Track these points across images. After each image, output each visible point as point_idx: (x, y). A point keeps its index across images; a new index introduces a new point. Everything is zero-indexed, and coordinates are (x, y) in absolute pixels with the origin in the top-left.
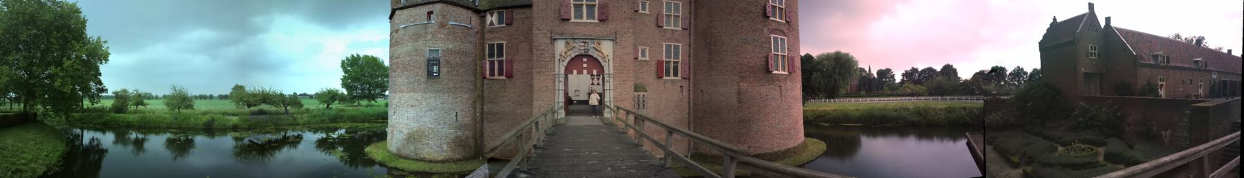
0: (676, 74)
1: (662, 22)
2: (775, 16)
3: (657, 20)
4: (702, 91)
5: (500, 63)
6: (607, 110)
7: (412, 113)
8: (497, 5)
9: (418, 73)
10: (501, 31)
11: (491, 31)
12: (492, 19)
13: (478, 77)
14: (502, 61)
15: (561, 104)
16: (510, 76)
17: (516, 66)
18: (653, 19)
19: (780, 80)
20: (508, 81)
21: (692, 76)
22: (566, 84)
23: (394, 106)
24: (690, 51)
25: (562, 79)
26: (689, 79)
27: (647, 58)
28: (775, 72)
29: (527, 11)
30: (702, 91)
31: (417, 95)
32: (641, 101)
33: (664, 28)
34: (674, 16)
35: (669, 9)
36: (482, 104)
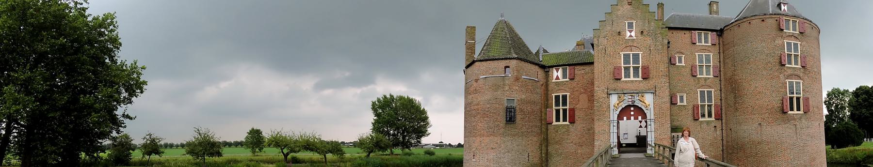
0: (710, 115)
1: (696, 72)
2: (790, 63)
4: (731, 129)
5: (565, 111)
7: (492, 155)
13: (543, 122)
14: (566, 109)
15: (615, 143)
16: (572, 121)
17: (577, 114)
18: (688, 70)
20: (571, 126)
22: (618, 128)
24: (721, 95)
25: (616, 124)
26: (722, 120)
30: (731, 129)
31: (496, 138)
33: (698, 76)
34: (706, 66)
35: (701, 61)
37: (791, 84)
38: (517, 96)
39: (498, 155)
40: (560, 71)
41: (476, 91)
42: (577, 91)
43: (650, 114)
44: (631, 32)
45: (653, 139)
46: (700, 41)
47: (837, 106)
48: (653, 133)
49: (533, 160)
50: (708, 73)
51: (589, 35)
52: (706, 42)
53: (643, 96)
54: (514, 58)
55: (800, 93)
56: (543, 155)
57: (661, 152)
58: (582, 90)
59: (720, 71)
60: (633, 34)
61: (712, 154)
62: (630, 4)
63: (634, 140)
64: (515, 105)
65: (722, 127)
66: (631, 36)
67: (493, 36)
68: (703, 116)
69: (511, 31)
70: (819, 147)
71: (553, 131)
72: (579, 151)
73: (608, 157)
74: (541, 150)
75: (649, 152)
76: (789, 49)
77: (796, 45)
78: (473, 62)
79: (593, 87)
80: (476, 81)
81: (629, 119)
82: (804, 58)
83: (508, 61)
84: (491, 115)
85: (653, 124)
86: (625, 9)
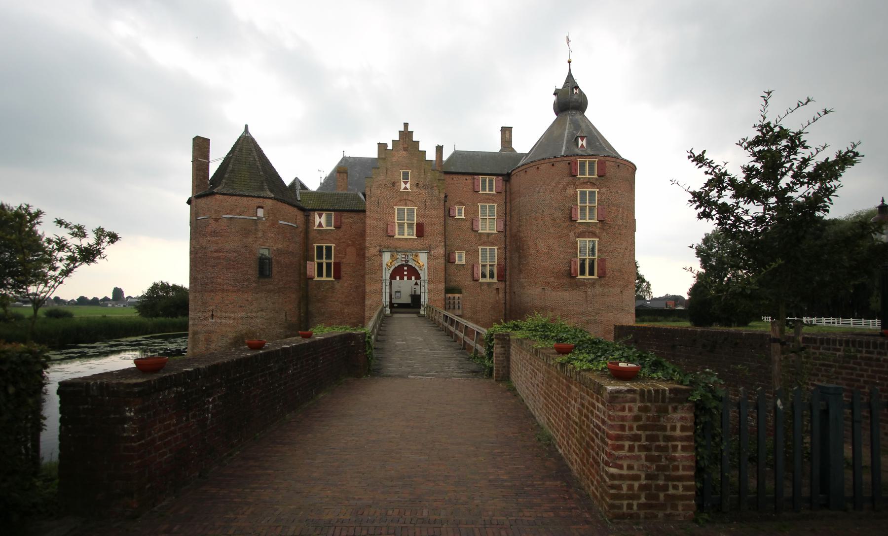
0: (492, 276)
3: (473, 224)
4: (514, 293)
5: (329, 265)
9: (247, 271)
10: (329, 233)
11: (320, 232)
14: (331, 263)
15: (387, 303)
16: (338, 276)
17: (344, 270)
20: (336, 283)
21: (508, 278)
25: (388, 284)
28: (580, 277)
31: (246, 296)
32: (456, 302)
39: (249, 314)
42: (344, 242)
43: (424, 275)
45: (426, 300)
48: (426, 294)
49: (291, 321)
56: (302, 315)
58: (350, 242)
61: (493, 318)
63: (406, 299)
65: (505, 290)
71: (315, 287)
72: (346, 311)
74: (300, 309)
75: (422, 312)
79: (364, 240)
81: (402, 278)
84: (239, 266)
85: (426, 284)
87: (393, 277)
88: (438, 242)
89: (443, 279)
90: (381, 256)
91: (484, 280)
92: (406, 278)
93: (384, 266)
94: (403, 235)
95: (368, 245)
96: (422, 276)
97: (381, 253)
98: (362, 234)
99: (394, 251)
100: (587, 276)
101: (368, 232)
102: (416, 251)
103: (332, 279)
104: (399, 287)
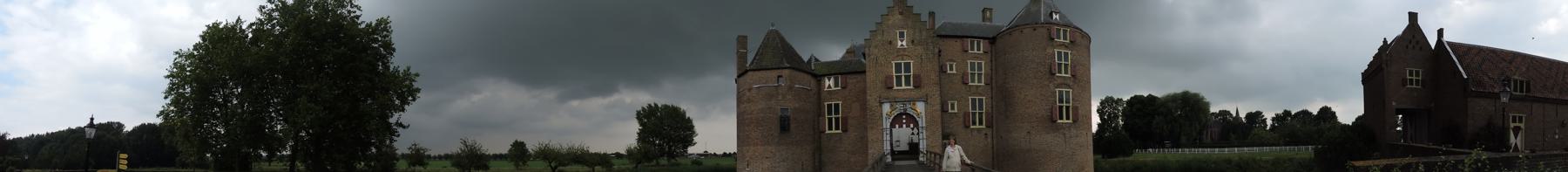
2: (1060, 72)
5: (837, 119)
6: (921, 155)
8: (833, 72)
12: (829, 83)
14: (838, 118)
16: (845, 130)
17: (850, 121)
19: (1064, 129)
22: (891, 136)
23: (748, 159)
25: (888, 132)
27: (956, 111)
28: (1059, 121)
29: (859, 77)
31: (770, 148)
35: (973, 68)
36: (820, 155)
37: (1061, 92)
38: (790, 104)
40: (832, 80)
41: (749, 101)
43: (922, 122)
44: (902, 41)
46: (972, 49)
47: (1110, 114)
50: (980, 81)
51: (860, 41)
52: (979, 50)
53: (914, 104)
54: (786, 68)
55: (1069, 103)
57: (932, 159)
59: (992, 79)
60: (904, 43)
62: (901, 13)
63: (906, 148)
64: (789, 114)
66: (902, 45)
67: (764, 46)
68: (974, 123)
69: (782, 40)
70: (1088, 156)
73: (883, 164)
75: (921, 159)
76: (1060, 59)
77: (1066, 54)
78: (746, 71)
80: (750, 90)
81: (901, 126)
82: (1074, 67)
83: (779, 71)
85: (924, 132)
86: (897, 18)
87: (892, 126)
88: (934, 92)
89: (940, 125)
90: (881, 106)
91: (974, 127)
92: (904, 126)
93: (884, 116)
94: (901, 86)
95: (868, 98)
96: (920, 123)
97: (881, 103)
98: (864, 92)
99: (893, 102)
100: (1065, 121)
101: (868, 85)
102: (913, 101)
103: (840, 131)
104: (898, 137)
